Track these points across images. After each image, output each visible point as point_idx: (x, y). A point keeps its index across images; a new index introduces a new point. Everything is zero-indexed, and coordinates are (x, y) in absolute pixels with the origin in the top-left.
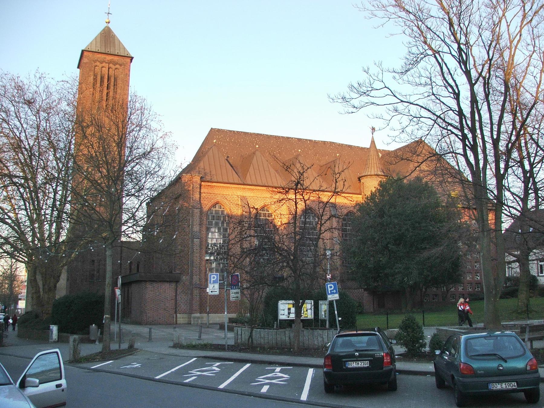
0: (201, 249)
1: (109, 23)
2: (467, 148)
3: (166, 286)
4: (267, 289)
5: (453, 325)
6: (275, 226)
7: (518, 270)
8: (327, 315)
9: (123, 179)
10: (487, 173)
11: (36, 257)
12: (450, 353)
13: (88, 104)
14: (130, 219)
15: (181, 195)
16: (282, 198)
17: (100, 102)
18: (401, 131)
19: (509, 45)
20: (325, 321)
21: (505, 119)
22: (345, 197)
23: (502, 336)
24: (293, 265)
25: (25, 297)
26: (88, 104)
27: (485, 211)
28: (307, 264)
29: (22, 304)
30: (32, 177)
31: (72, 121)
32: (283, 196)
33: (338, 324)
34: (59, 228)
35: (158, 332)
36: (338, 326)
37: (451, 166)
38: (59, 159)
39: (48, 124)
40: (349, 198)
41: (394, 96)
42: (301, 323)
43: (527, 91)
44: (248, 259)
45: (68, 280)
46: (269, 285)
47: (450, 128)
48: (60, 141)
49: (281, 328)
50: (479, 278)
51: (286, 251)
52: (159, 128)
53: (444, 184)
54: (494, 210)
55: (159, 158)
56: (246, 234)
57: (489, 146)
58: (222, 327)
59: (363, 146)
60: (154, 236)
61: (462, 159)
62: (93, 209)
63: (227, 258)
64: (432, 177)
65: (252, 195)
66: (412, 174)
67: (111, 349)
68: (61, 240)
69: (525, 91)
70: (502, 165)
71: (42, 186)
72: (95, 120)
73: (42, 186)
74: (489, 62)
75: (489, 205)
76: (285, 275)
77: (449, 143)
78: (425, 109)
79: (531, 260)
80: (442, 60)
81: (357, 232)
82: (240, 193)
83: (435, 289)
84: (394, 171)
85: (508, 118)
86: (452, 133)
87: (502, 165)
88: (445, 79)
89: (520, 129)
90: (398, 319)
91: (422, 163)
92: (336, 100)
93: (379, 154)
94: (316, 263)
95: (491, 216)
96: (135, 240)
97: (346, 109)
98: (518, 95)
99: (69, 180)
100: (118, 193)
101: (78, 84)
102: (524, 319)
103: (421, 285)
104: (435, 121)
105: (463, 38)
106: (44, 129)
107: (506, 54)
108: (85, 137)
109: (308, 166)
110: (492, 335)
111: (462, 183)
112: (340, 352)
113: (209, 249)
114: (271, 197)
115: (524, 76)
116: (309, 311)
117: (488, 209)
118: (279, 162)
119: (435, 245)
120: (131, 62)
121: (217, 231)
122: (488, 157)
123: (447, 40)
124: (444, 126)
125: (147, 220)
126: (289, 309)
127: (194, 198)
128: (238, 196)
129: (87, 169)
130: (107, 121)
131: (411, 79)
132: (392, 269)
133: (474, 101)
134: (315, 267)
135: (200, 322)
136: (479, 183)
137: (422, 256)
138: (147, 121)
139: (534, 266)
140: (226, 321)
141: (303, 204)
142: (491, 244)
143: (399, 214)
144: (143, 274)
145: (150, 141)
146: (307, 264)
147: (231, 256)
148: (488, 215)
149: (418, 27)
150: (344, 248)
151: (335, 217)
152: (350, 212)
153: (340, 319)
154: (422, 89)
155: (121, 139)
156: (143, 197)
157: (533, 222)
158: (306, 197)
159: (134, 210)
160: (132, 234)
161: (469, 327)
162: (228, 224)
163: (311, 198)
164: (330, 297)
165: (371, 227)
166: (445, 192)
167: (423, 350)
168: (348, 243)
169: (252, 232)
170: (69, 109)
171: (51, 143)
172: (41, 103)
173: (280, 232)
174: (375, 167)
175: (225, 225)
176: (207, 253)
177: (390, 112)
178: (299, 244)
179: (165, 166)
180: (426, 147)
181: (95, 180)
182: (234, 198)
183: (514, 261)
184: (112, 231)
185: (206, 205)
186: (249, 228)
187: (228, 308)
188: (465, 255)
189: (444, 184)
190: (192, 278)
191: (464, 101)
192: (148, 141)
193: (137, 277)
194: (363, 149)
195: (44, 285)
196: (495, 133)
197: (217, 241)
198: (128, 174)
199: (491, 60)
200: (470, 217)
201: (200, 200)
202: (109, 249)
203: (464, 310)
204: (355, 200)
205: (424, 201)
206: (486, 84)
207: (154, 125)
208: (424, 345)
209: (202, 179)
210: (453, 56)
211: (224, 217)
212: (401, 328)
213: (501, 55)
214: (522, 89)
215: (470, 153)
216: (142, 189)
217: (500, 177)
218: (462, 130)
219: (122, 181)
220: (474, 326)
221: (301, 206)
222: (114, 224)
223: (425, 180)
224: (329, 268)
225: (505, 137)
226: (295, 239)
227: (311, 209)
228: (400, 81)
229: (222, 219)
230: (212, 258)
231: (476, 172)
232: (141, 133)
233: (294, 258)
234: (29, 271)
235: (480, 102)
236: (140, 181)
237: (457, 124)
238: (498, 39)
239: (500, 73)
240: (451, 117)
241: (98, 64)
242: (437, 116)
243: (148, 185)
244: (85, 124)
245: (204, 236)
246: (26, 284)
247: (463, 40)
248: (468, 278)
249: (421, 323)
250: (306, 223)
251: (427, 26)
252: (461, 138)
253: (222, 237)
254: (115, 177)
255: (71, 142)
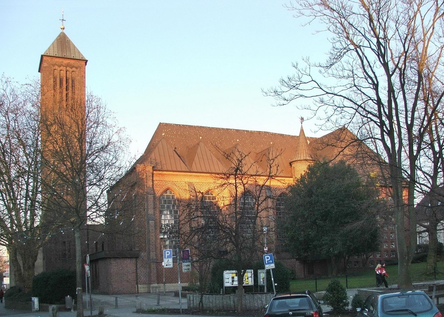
0: (156, 229)
1: (64, 29)
2: (385, 133)
3: (128, 261)
4: (213, 261)
5: (372, 286)
6: (218, 207)
7: (428, 239)
8: (265, 281)
9: (85, 171)
10: (402, 155)
11: (15, 240)
12: (369, 310)
13: (50, 105)
14: (93, 205)
15: (136, 183)
16: (224, 183)
17: (60, 102)
18: (326, 120)
19: (423, 37)
20: (263, 286)
21: (418, 106)
22: (278, 180)
23: (413, 294)
24: (235, 240)
25: (9, 275)
26: (50, 105)
27: (399, 189)
28: (247, 239)
29: (6, 281)
30: (6, 172)
31: (37, 121)
32: (224, 181)
33: (274, 289)
34: (33, 215)
35: (123, 300)
36: (275, 290)
37: (370, 149)
38: (29, 155)
39: (16, 124)
40: (282, 181)
41: (320, 88)
42: (244, 289)
43: (438, 80)
44: (196, 237)
45: (44, 259)
46: (214, 258)
47: (369, 116)
48: (28, 138)
49: (226, 293)
50: (394, 246)
51: (229, 228)
52: (114, 124)
53: (364, 166)
54: (408, 187)
55: (115, 151)
56: (194, 215)
57: (404, 131)
58: (176, 294)
59: (294, 135)
60: (115, 219)
61: (380, 144)
62: (61, 198)
63: (178, 237)
64: (353, 160)
65: (198, 181)
66: (337, 158)
67: (85, 316)
68: (35, 225)
69: (436, 80)
70: (415, 148)
71: (16, 179)
72: (57, 118)
73: (16, 179)
74: (404, 54)
75: (403, 183)
76: (228, 249)
77: (369, 129)
78: (348, 99)
79: (438, 230)
80: (363, 54)
81: (289, 210)
82: (187, 180)
83: (356, 257)
84: (320, 156)
85: (421, 105)
86: (372, 120)
87: (415, 148)
88: (365, 71)
89: (431, 115)
90: (325, 283)
91: (345, 148)
92: (268, 94)
93: (308, 141)
94: (255, 238)
95: (405, 193)
96: (99, 224)
97: (278, 102)
98: (430, 84)
99: (39, 173)
100: (81, 183)
101: (40, 86)
102: (431, 280)
103: (345, 254)
104: (356, 110)
105: (382, 33)
106: (13, 128)
107: (420, 47)
108: (49, 134)
109: (246, 154)
110: (404, 294)
111: (380, 165)
112: (277, 312)
113: (163, 229)
114: (214, 182)
115: (436, 66)
116: (250, 279)
117: (403, 187)
118: (220, 151)
119: (357, 219)
120: (86, 64)
121: (169, 213)
122: (403, 141)
123: (367, 35)
124: (364, 114)
125: (109, 206)
126: (233, 278)
127: (148, 186)
128: (185, 182)
129: (54, 163)
130: (68, 119)
131: (335, 72)
132: (320, 241)
133: (391, 90)
134: (254, 242)
135: (157, 290)
136: (394, 165)
137: (345, 229)
138: (103, 118)
139: (441, 235)
140: (180, 289)
141: (243, 188)
142: (405, 217)
143: (325, 193)
144: (107, 252)
145: (107, 136)
146: (247, 239)
147: (182, 235)
148: (402, 192)
149: (341, 24)
150: (279, 225)
151: (270, 198)
152: (283, 193)
153: (276, 284)
154: (345, 81)
155: (81, 135)
156: (103, 186)
157: (441, 197)
158: (245, 181)
159: (97, 198)
160: (96, 218)
161: (385, 287)
162: (178, 207)
163: (249, 182)
164: (267, 267)
165: (301, 205)
166: (365, 173)
167: (346, 308)
168: (282, 220)
169: (199, 214)
170: (34, 110)
171: (20, 140)
172: (8, 105)
173: (223, 212)
174: (304, 153)
175: (176, 208)
176: (161, 232)
177: (317, 103)
178: (240, 222)
179: (121, 158)
180: (349, 134)
181: (61, 172)
182: (182, 184)
183: (424, 231)
184: (78, 216)
185: (159, 191)
186: (196, 210)
187: (181, 279)
188: (382, 227)
189: (364, 166)
190: (149, 254)
191: (382, 90)
192: (105, 136)
193: (103, 255)
194: (293, 137)
195: (24, 264)
196: (409, 119)
197: (169, 221)
198: (90, 166)
199: (406, 53)
200: (386, 194)
201: (153, 187)
202: (77, 231)
203: (381, 274)
204: (287, 182)
205: (347, 182)
206: (402, 75)
207: (109, 122)
208: (347, 304)
209: (154, 169)
210: (372, 49)
211: (175, 201)
212: (327, 291)
213: (416, 47)
214: (433, 78)
215: (387, 139)
216: (103, 179)
217: (413, 158)
218: (380, 117)
219: (85, 173)
220: (389, 287)
221: (241, 189)
222: (80, 210)
223: (348, 163)
224: (265, 242)
225: (418, 122)
226: (236, 218)
227: (249, 191)
228: (326, 74)
229: (173, 203)
230: (166, 237)
231: (393, 155)
232: (99, 130)
233: (236, 234)
234: (10, 252)
235: (396, 91)
236: (100, 172)
237: (376, 112)
238: (413, 33)
239: (414, 64)
240: (370, 106)
241: (56, 67)
242: (358, 105)
243: (107, 175)
244: (49, 123)
245: (158, 218)
246: (8, 263)
247: (381, 35)
248: (385, 247)
249: (344, 286)
250: (246, 203)
251: (349, 23)
252: (379, 124)
253: (173, 218)
254: (78, 169)
255: (38, 139)
